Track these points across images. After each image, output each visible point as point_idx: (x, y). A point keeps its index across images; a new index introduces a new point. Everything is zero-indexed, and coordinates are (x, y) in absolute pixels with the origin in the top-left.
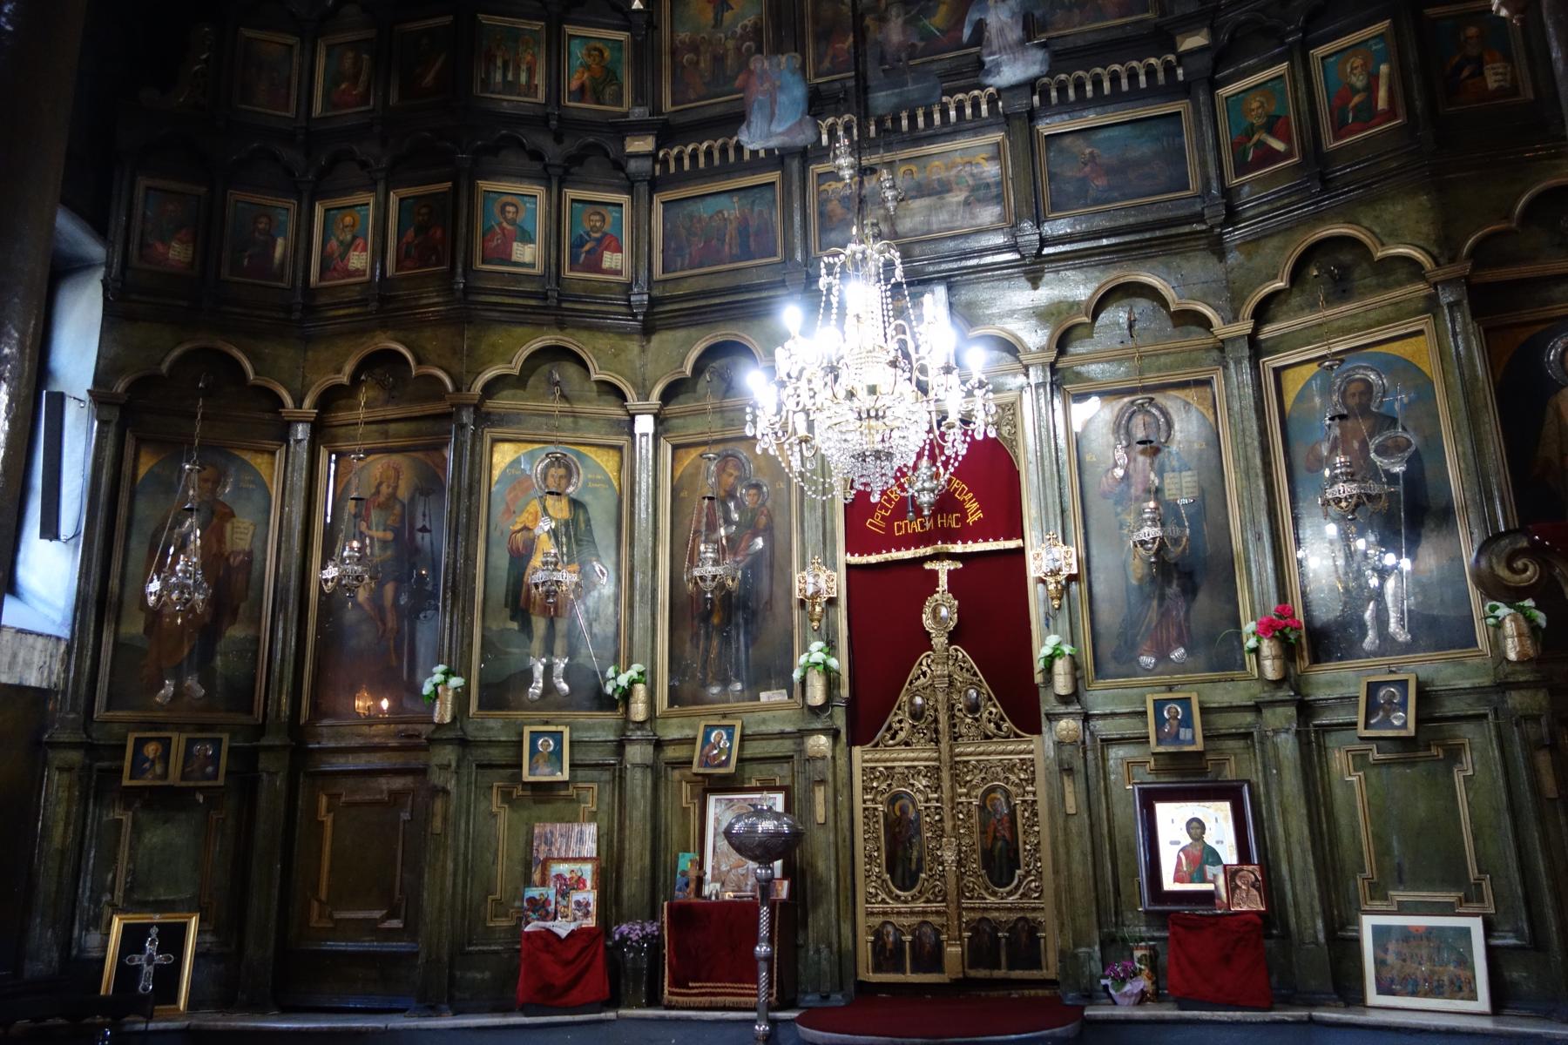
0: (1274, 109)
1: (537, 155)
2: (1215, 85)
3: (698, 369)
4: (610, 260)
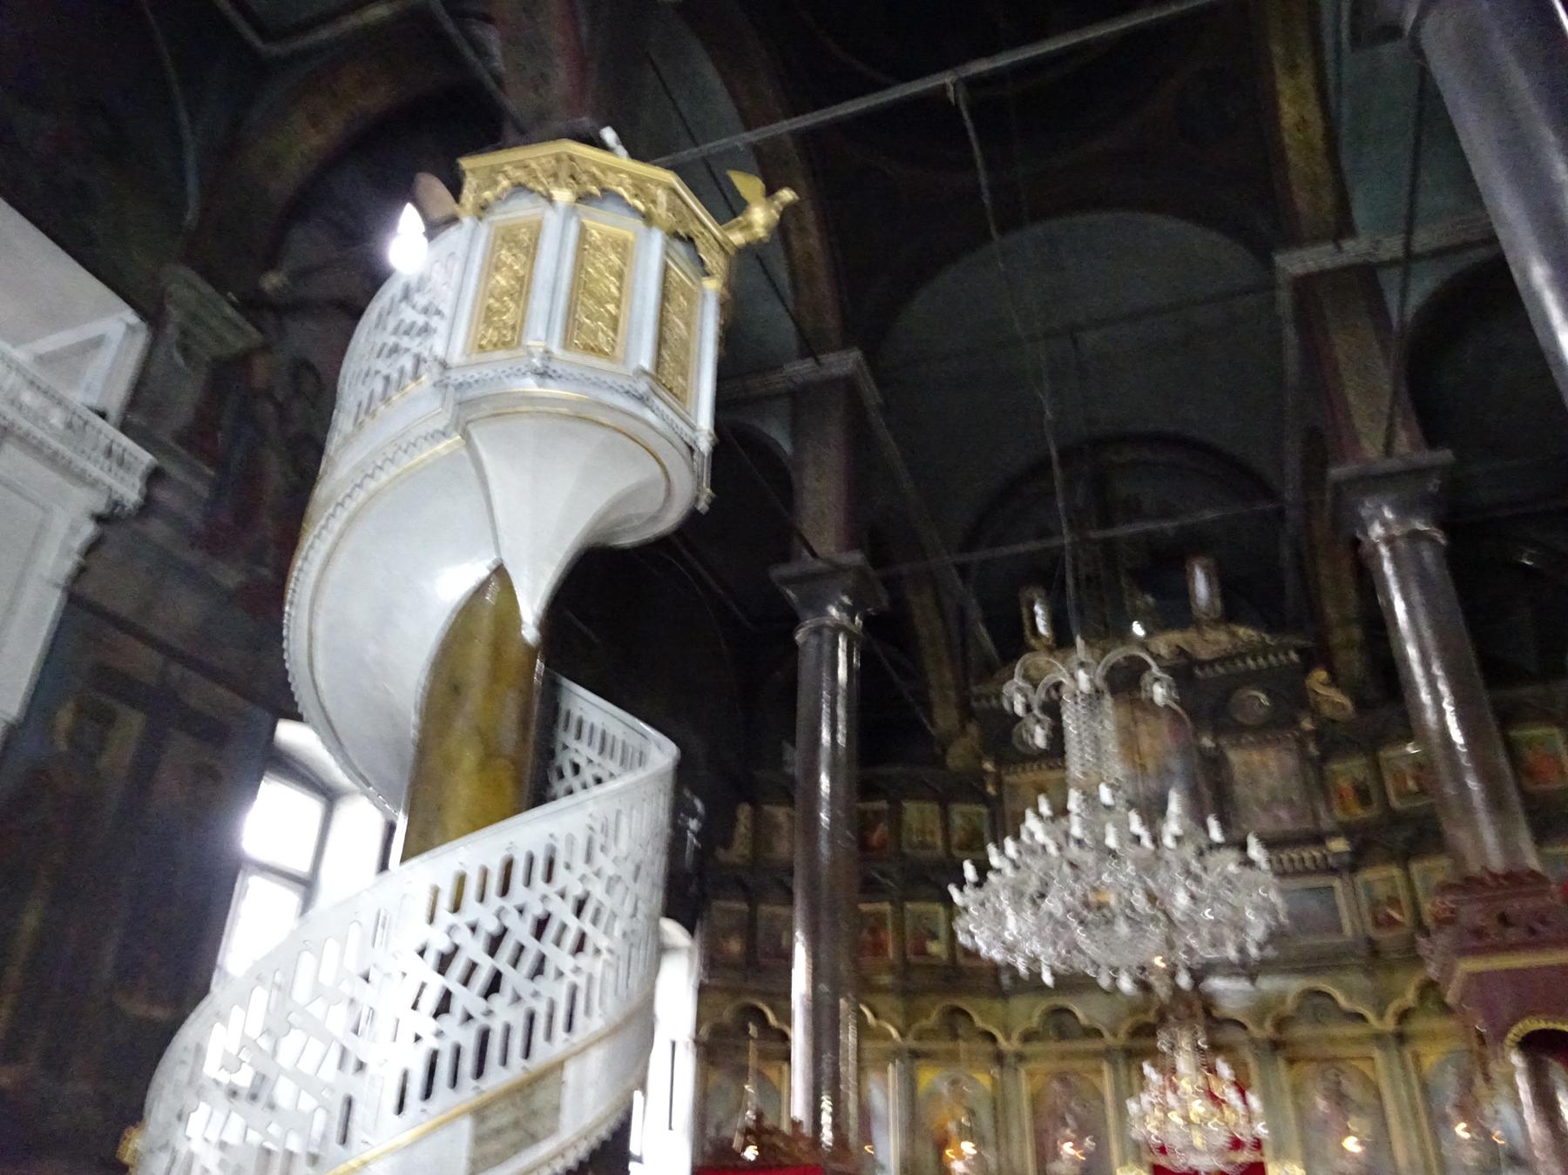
2: (1354, 868)
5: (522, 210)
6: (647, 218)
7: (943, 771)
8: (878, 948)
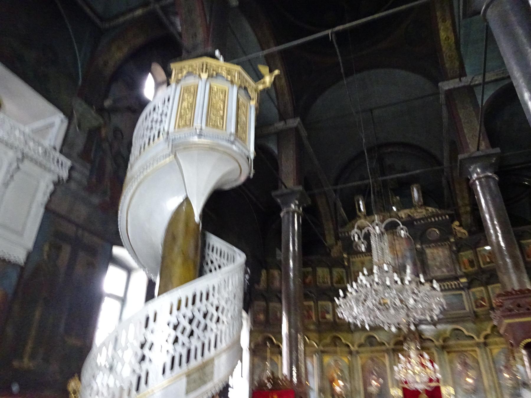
2: (469, 288)
5: (191, 81)
6: (232, 82)
7: (330, 260)
8: (310, 317)
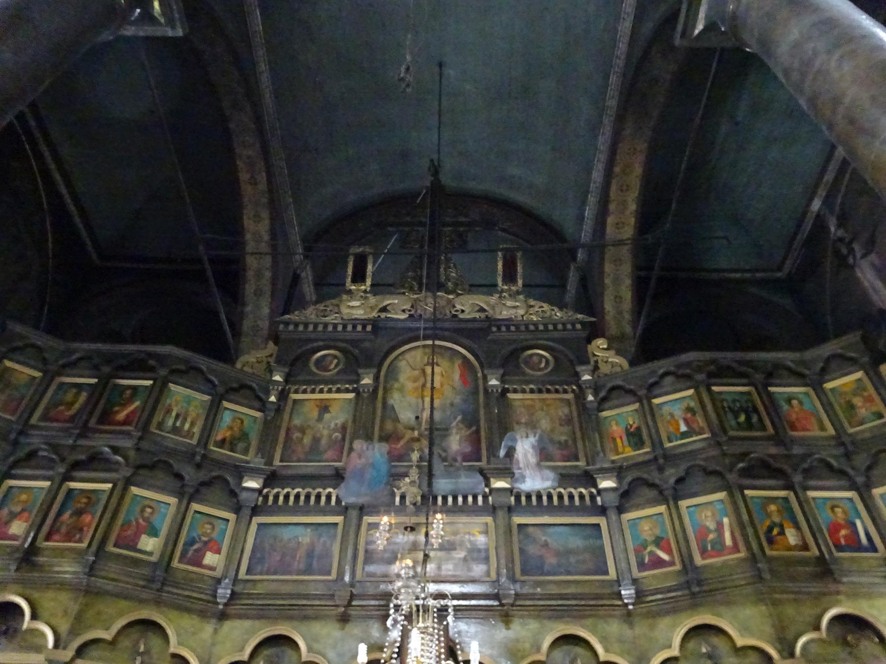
0: (658, 532)
1: (179, 476)
2: (621, 510)
3: (253, 655)
4: (210, 558)
